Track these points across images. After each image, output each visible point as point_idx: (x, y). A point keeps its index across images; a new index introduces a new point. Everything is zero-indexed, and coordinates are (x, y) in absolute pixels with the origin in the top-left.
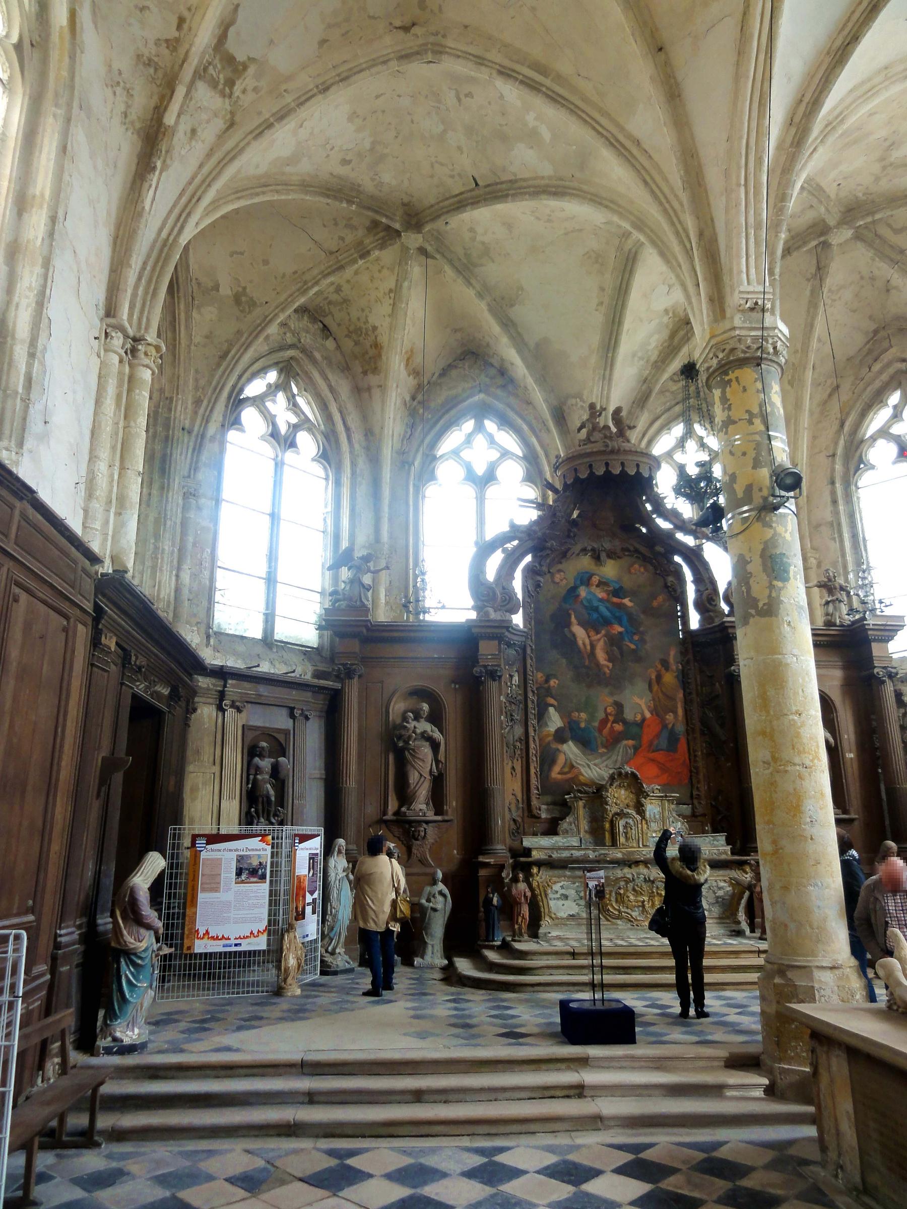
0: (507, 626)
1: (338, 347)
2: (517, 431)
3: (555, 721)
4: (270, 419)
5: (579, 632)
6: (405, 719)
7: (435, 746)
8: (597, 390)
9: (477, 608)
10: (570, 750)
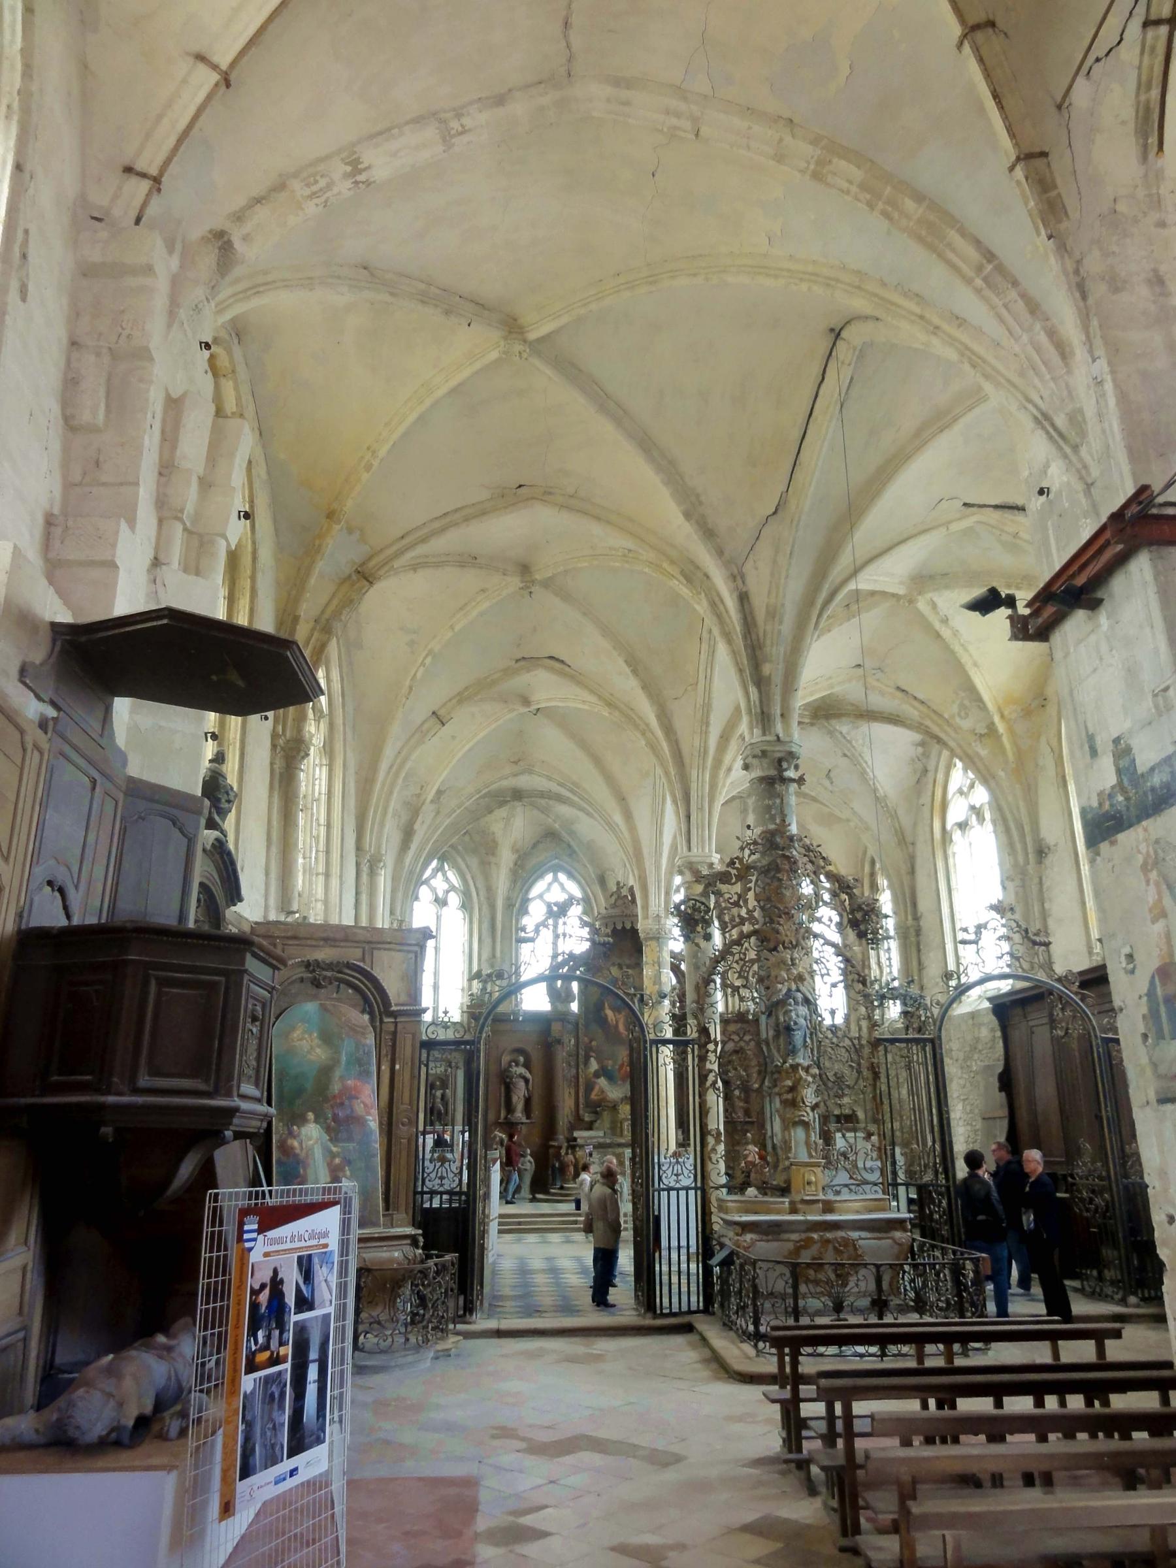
0: (568, 1013)
1: (471, 838)
2: (579, 883)
3: (594, 1065)
4: (434, 890)
5: (609, 1013)
6: (510, 1066)
7: (527, 1081)
8: (621, 872)
9: (552, 1003)
10: (602, 1082)
